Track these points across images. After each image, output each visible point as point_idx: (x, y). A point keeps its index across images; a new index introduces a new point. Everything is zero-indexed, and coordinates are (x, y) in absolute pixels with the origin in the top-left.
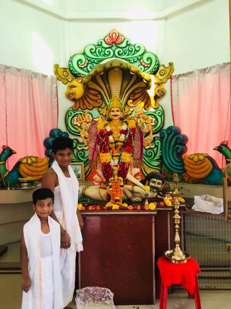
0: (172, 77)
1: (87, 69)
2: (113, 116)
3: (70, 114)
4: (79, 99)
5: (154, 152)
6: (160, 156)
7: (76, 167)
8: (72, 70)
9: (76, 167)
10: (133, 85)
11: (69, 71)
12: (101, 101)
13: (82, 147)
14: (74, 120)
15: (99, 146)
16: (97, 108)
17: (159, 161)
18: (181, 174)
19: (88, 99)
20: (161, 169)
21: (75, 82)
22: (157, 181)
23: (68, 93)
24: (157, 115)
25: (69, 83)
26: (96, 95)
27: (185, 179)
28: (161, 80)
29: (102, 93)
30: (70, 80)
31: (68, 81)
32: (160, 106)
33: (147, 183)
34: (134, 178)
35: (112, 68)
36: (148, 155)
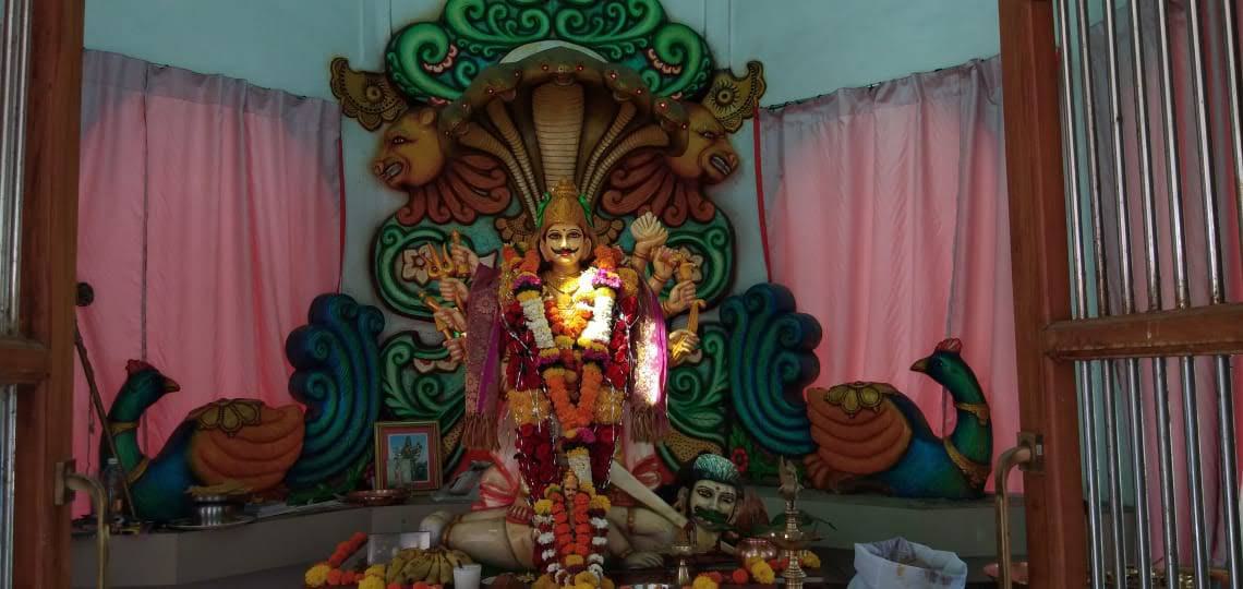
0: (759, 110)
1: (456, 80)
2: (556, 252)
3: (388, 241)
4: (424, 187)
5: (700, 376)
6: (722, 392)
7: (408, 438)
8: (399, 82)
9: (408, 438)
10: (624, 139)
11: (386, 83)
12: (504, 193)
13: (433, 363)
14: (404, 263)
15: (504, 366)
16: (491, 219)
17: (718, 412)
18: (800, 457)
19: (458, 186)
20: (728, 441)
21: (409, 126)
22: (718, 488)
23: (384, 162)
24: (710, 244)
25: (385, 126)
26: (487, 173)
27: (815, 475)
28: (719, 121)
29: (511, 163)
30: (389, 115)
31: (383, 120)
32: (719, 213)
33: (681, 496)
34: (633, 478)
35: (551, 78)
36: (680, 388)
